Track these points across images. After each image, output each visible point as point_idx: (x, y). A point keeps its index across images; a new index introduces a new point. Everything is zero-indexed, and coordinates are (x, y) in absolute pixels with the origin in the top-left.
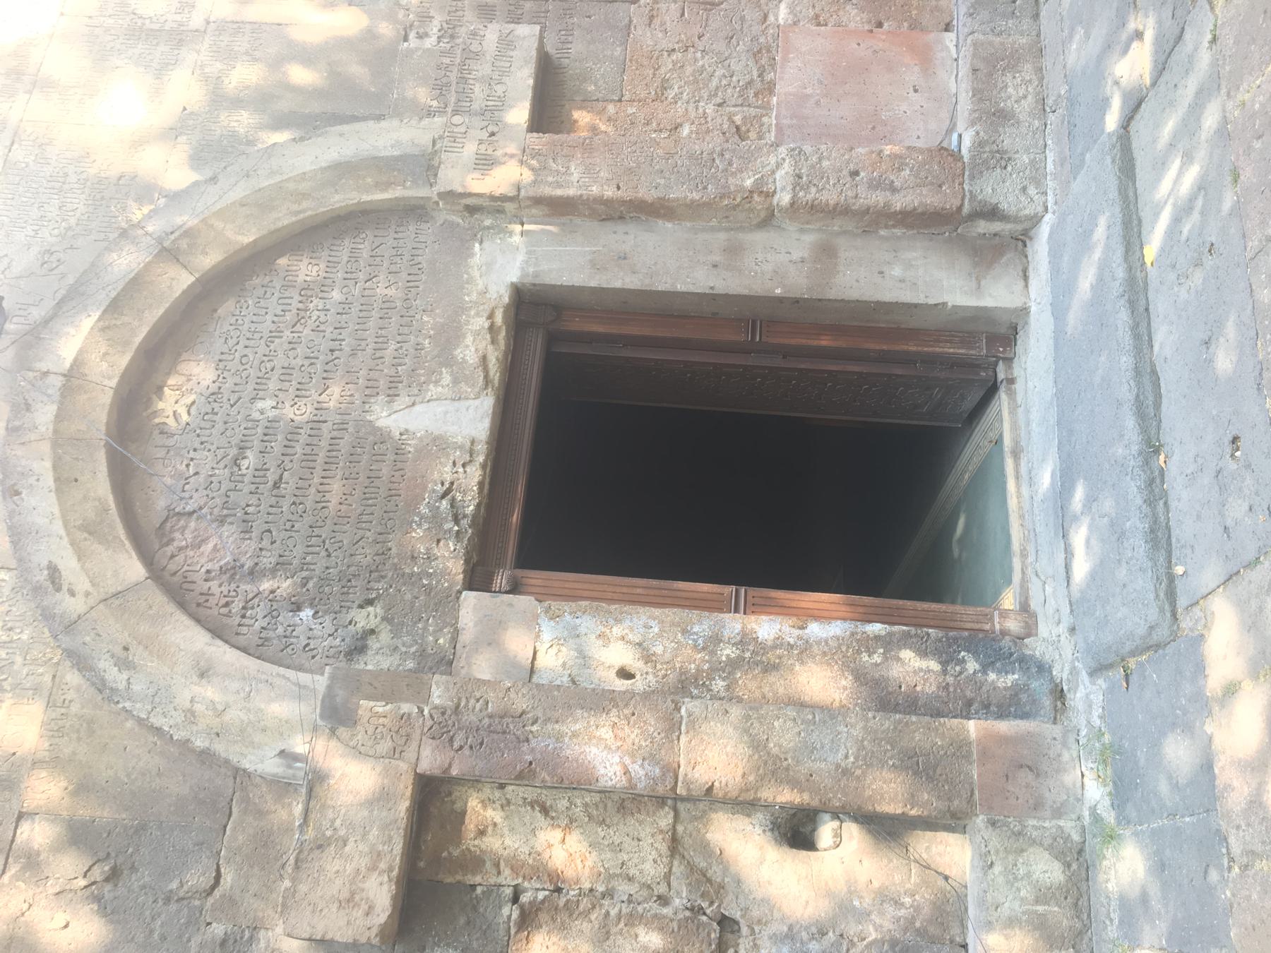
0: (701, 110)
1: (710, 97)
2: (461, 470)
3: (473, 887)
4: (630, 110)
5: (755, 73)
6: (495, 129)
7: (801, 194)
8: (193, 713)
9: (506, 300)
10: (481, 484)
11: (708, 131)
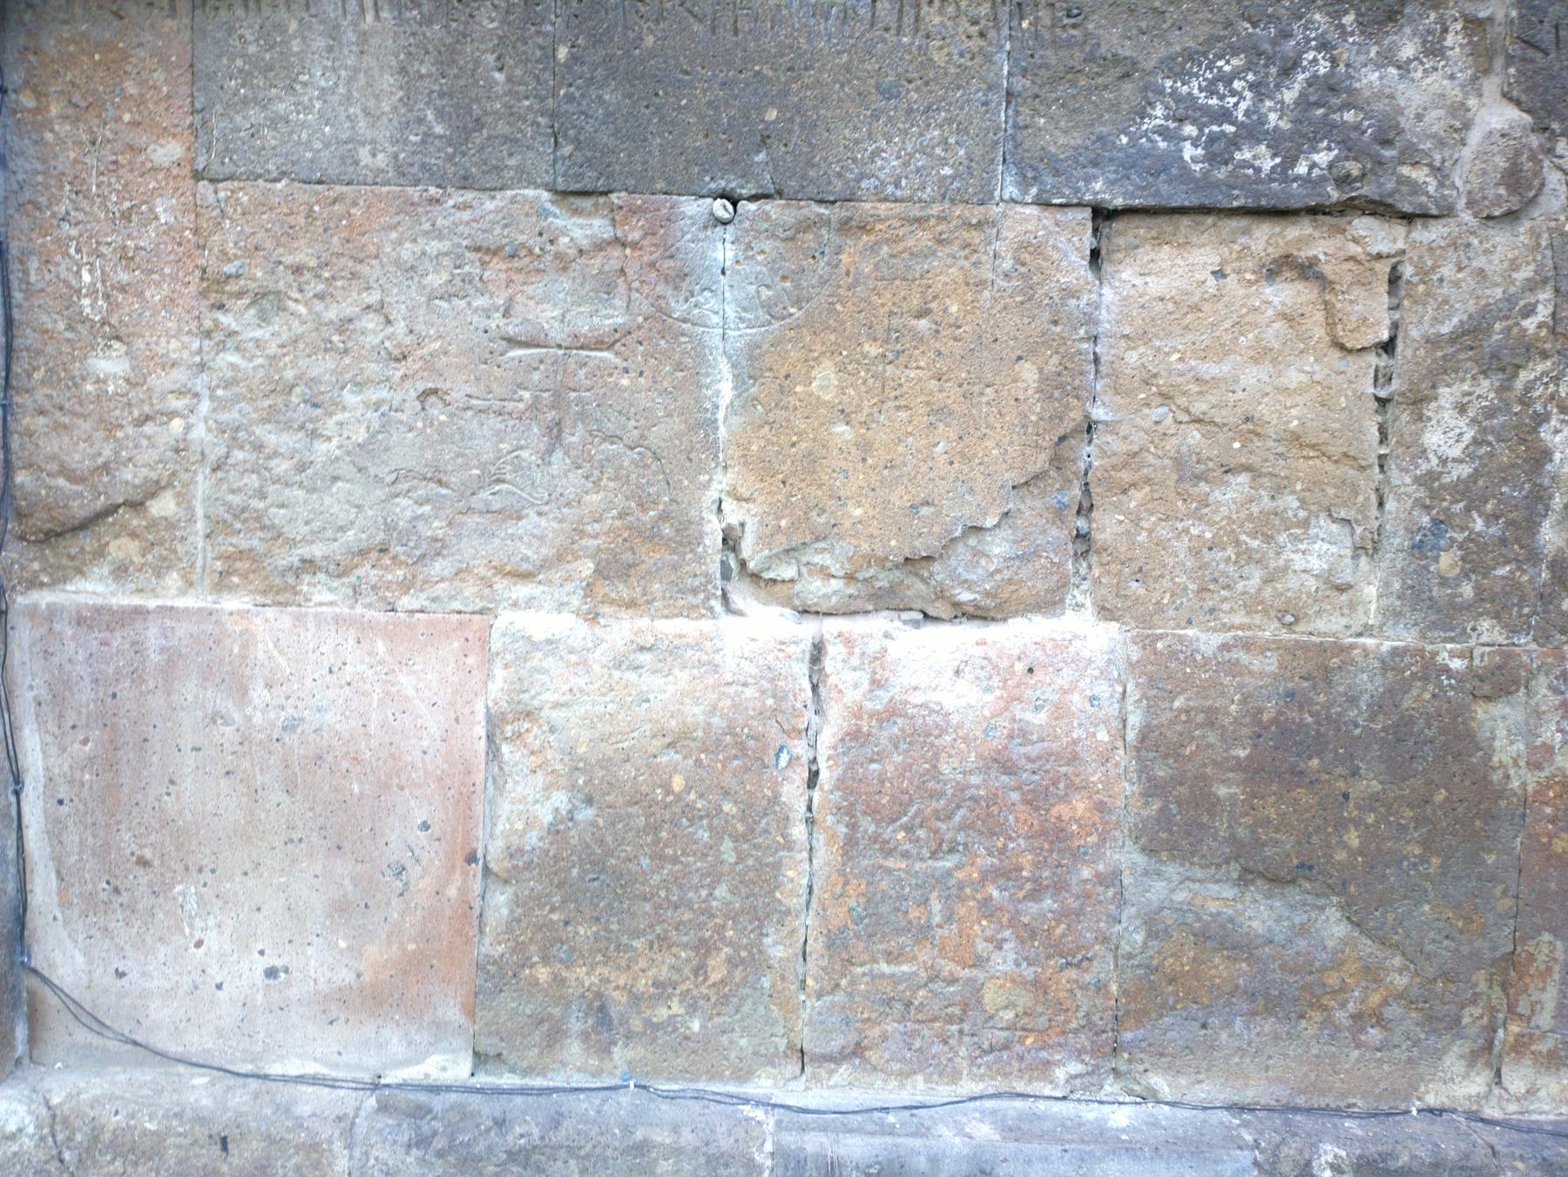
4: (164, 210)
5: (317, 551)
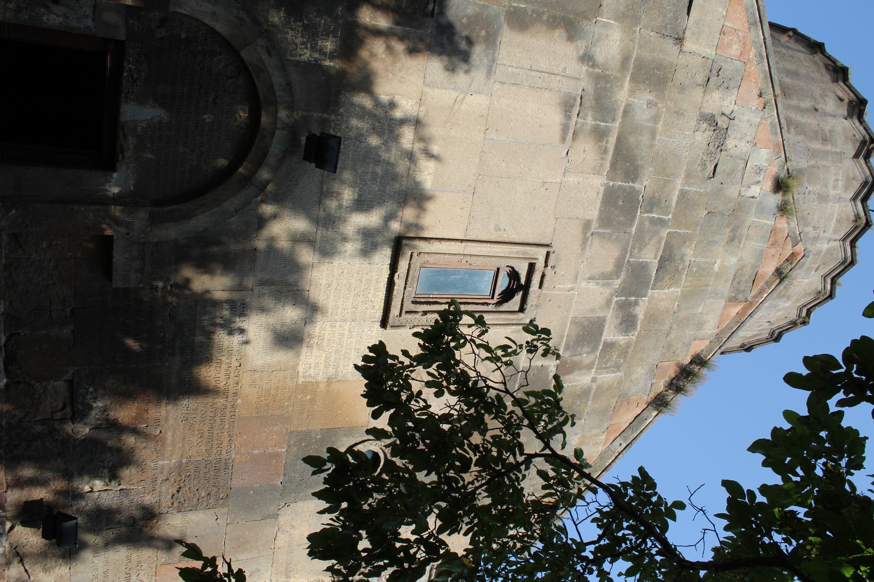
9: (118, 165)
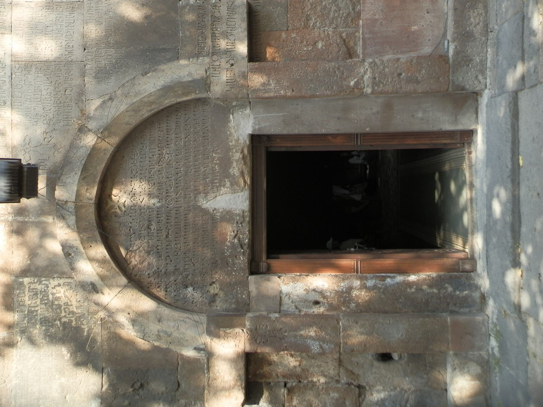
0: (326, 33)
1: (331, 23)
2: (240, 225)
3: (270, 383)
5: (351, 8)
6: (233, 62)
7: (376, 88)
8: (160, 336)
9: (248, 142)
10: (249, 231)
11: (331, 44)
